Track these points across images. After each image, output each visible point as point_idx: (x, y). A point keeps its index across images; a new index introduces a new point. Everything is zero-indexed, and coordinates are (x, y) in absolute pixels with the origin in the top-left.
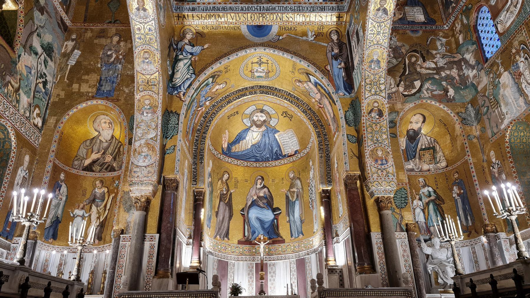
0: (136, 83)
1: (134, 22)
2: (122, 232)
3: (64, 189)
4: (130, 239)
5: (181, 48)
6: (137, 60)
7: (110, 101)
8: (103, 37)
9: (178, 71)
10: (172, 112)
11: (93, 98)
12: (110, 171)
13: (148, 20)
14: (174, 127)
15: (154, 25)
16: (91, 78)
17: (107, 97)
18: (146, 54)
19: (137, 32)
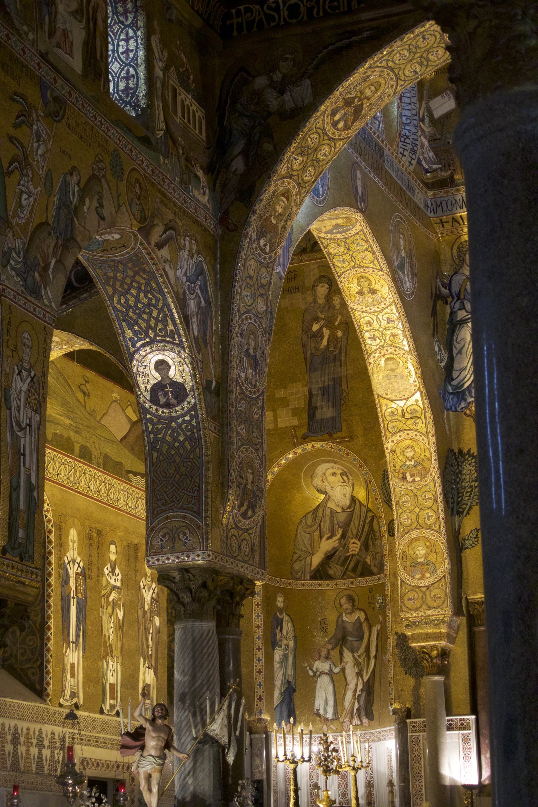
0: (380, 419)
1: (357, 313)
2: (409, 716)
3: (287, 626)
4: (425, 726)
5: (459, 293)
6: (375, 376)
7: (336, 443)
8: (297, 288)
9: (460, 352)
10: (461, 452)
11: (305, 439)
12: (362, 575)
13: (383, 306)
14: (471, 487)
15: (395, 311)
16: (291, 394)
17: (330, 435)
18: (391, 362)
19: (366, 329)
